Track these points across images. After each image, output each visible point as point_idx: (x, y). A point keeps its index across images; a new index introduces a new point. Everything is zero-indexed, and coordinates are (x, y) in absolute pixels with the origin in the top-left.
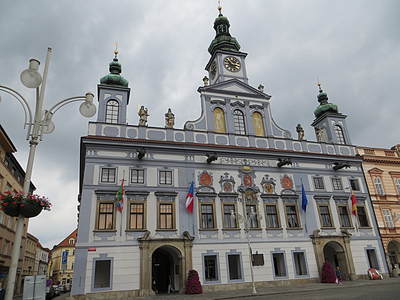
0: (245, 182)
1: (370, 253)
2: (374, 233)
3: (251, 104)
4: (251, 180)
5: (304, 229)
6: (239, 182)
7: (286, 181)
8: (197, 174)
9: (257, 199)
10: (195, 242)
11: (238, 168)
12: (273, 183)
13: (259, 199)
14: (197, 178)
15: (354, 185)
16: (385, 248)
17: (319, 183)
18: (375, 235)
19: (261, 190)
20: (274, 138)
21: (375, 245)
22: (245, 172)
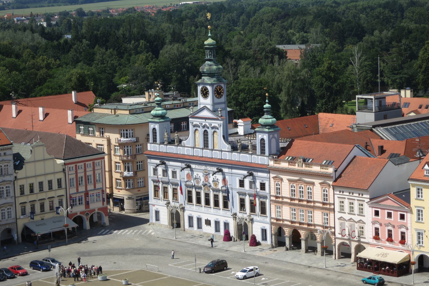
0: (205, 179)
1: (264, 231)
2: (268, 220)
3: (213, 125)
4: (208, 179)
5: (230, 210)
6: (202, 179)
7: (224, 180)
8: (186, 174)
9: (209, 190)
10: (186, 209)
11: (202, 171)
12: (218, 181)
13: (211, 190)
14: (186, 176)
15: (263, 186)
16: (272, 230)
17: (242, 184)
18: (268, 221)
19: (212, 185)
20: (222, 151)
21: (267, 227)
22: (205, 173)
